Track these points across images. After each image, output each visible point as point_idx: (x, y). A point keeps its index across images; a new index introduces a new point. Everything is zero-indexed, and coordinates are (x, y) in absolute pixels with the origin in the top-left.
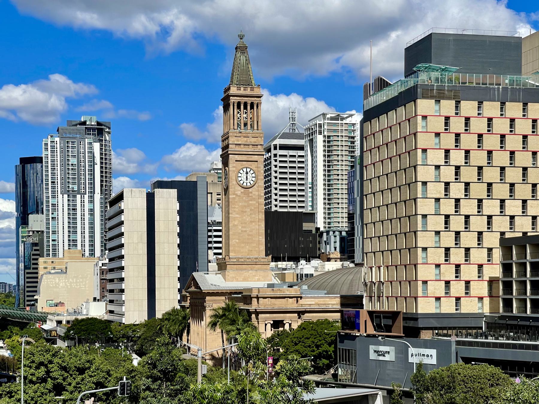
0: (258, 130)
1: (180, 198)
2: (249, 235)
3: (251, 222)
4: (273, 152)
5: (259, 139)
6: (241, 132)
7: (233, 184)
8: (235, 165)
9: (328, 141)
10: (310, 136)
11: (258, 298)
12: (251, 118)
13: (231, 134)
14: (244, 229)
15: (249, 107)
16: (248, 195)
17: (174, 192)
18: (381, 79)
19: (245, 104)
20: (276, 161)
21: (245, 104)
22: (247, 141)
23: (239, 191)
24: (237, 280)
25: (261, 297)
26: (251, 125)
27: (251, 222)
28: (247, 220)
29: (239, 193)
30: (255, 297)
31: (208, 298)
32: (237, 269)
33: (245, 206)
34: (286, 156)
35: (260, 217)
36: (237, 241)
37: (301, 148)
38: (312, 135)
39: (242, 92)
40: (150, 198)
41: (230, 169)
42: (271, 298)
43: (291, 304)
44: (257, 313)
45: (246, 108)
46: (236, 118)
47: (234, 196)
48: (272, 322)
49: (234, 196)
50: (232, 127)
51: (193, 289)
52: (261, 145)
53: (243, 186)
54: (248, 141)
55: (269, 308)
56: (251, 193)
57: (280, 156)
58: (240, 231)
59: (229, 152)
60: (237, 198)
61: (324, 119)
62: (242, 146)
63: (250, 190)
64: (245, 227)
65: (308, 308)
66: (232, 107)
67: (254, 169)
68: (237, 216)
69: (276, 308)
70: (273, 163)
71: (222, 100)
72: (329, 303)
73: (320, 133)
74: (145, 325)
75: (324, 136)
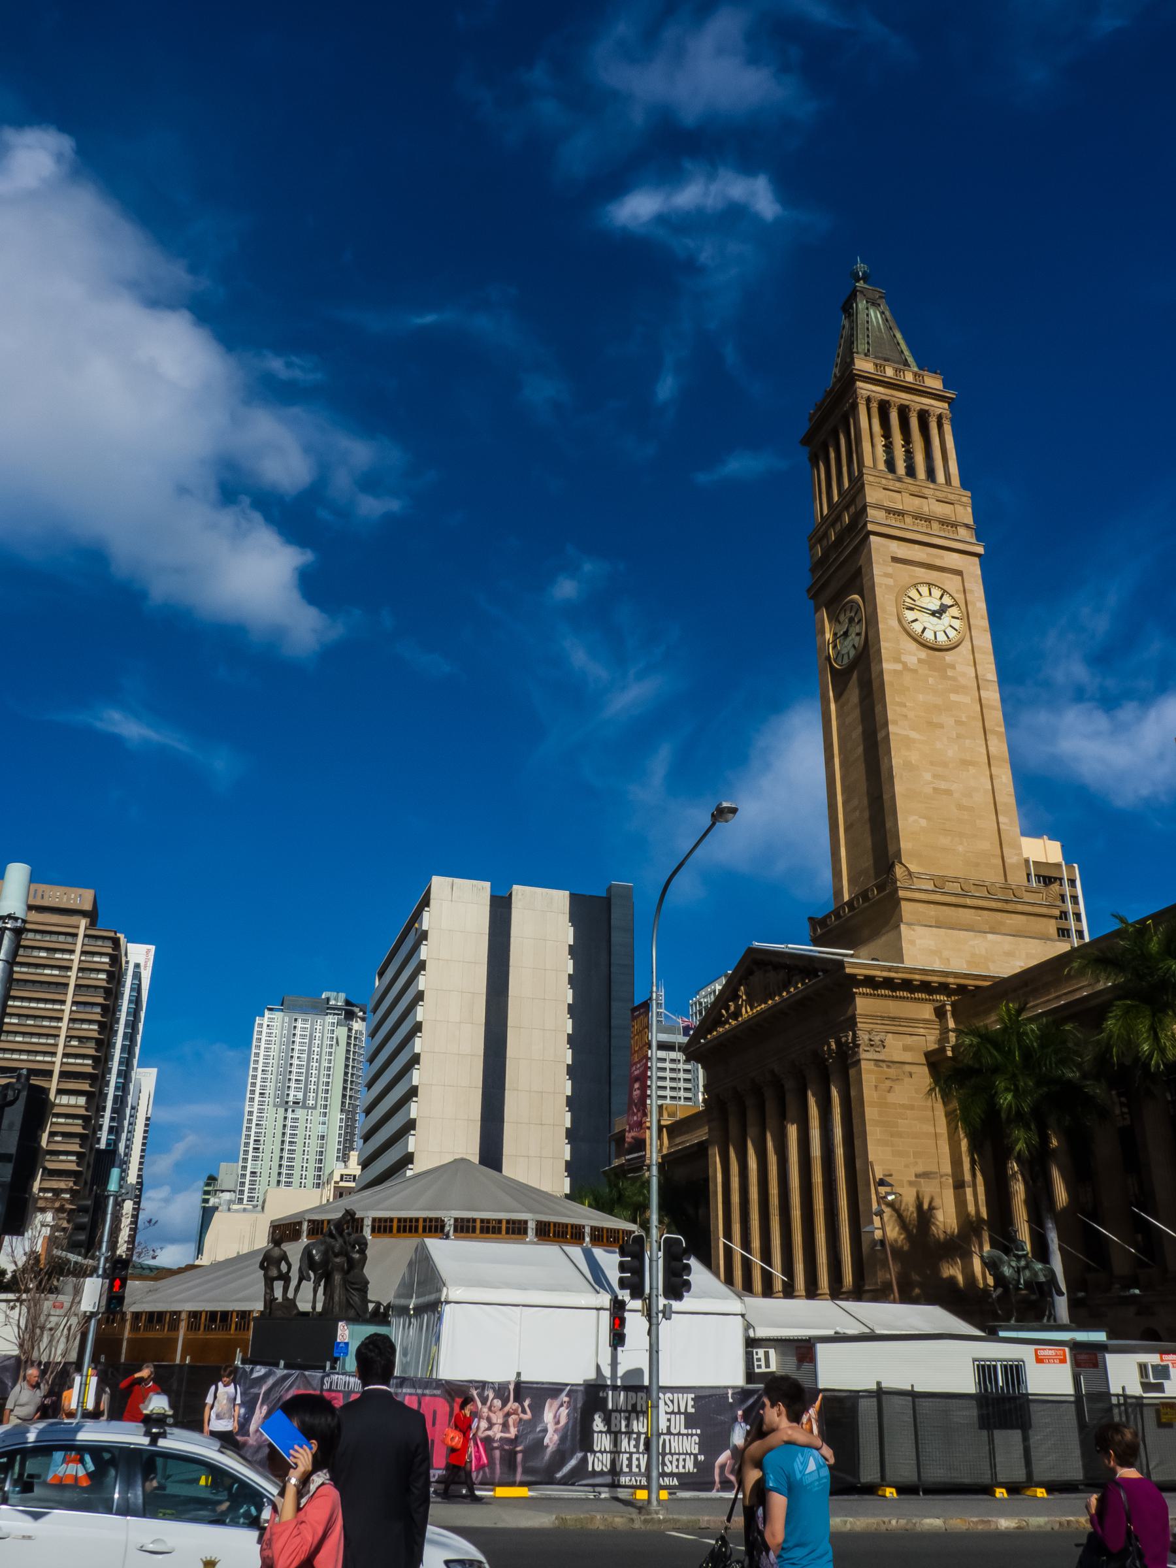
1: (576, 917)
2: (960, 807)
3: (965, 763)
5: (959, 508)
8: (890, 570)
13: (871, 479)
14: (943, 785)
16: (943, 670)
17: (561, 898)
19: (904, 411)
21: (904, 411)
23: (913, 655)
27: (965, 763)
28: (950, 753)
36: (923, 823)
40: (501, 910)
47: (899, 667)
49: (899, 667)
52: (967, 526)
58: (928, 790)
60: (907, 679)
62: (908, 520)
63: (949, 657)
68: (913, 735)
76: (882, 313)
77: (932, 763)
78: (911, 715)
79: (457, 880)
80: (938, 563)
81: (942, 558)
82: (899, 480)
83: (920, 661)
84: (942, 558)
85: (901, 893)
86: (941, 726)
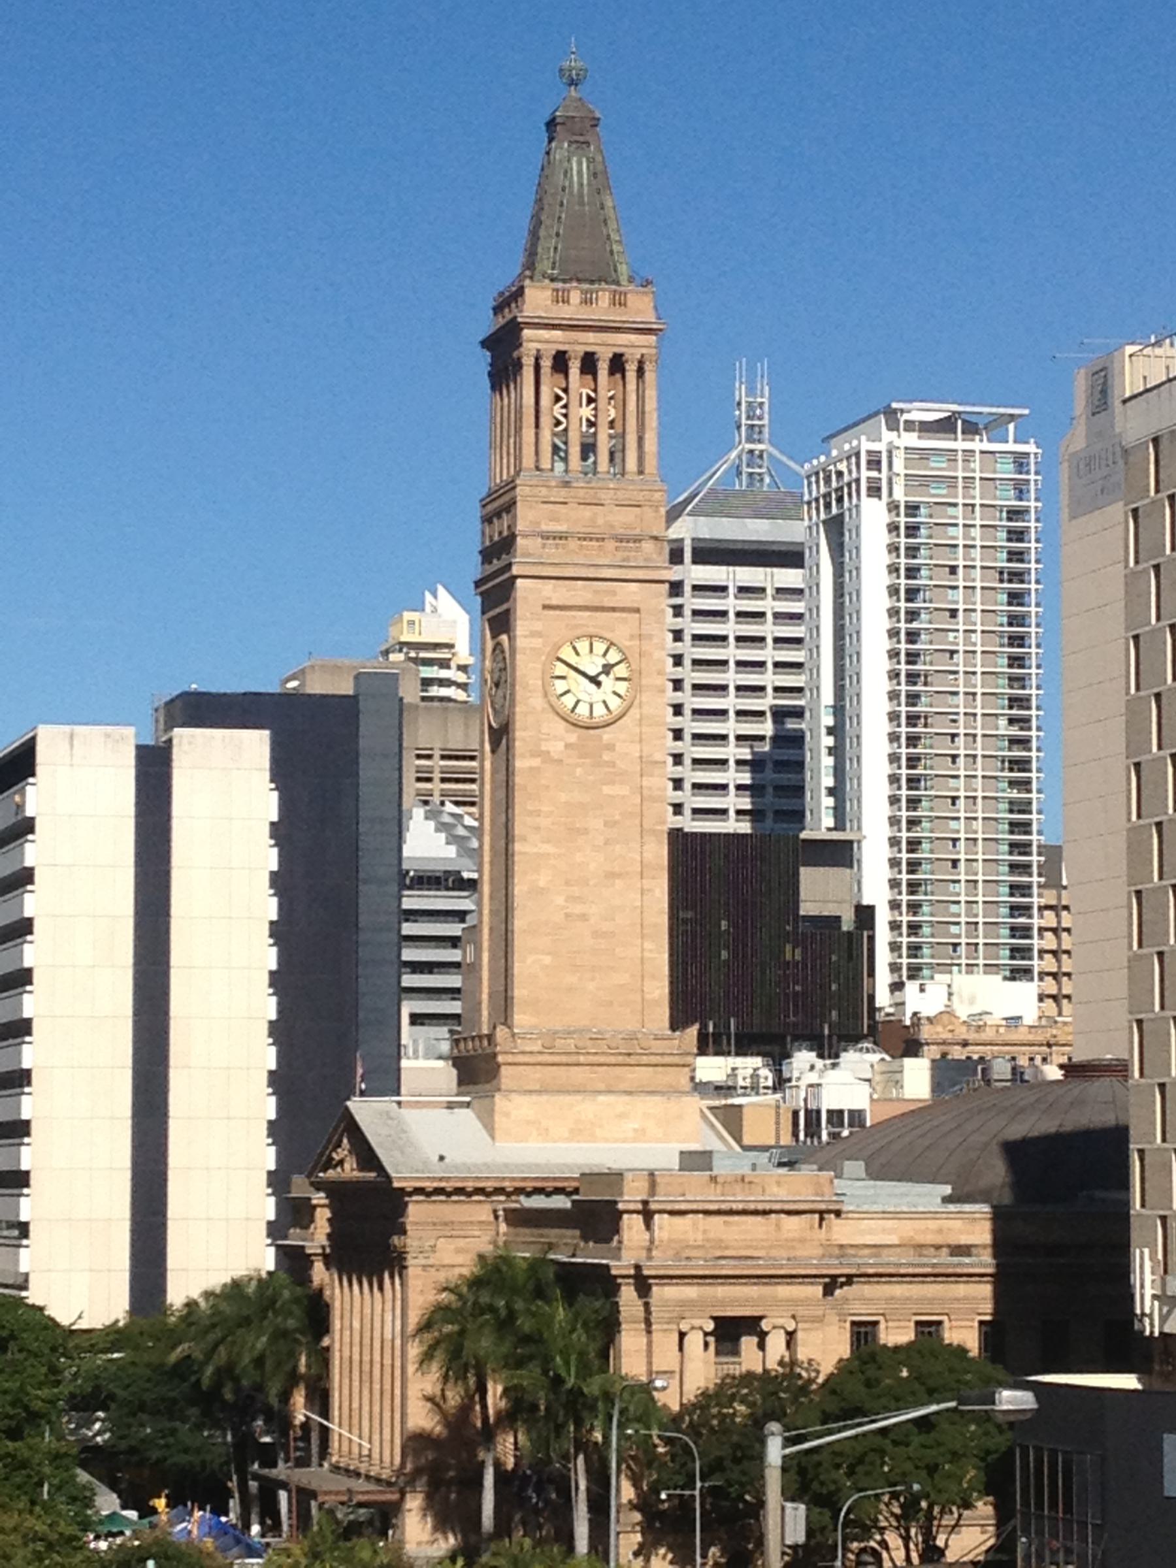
3: (612, 875)
5: (648, 512)
8: (538, 626)
12: (612, 424)
14: (578, 909)
26: (612, 454)
27: (612, 875)
29: (556, 748)
39: (573, 310)
46: (546, 422)
49: (536, 762)
50: (528, 460)
51: (349, 1170)
53: (573, 718)
54: (600, 521)
56: (610, 747)
59: (515, 570)
63: (607, 735)
71: (484, 344)
77: (567, 883)
78: (544, 822)
80: (607, 602)
81: (614, 593)
82: (566, 484)
83: (568, 746)
84: (614, 593)
85: (500, 1059)
86: (586, 831)
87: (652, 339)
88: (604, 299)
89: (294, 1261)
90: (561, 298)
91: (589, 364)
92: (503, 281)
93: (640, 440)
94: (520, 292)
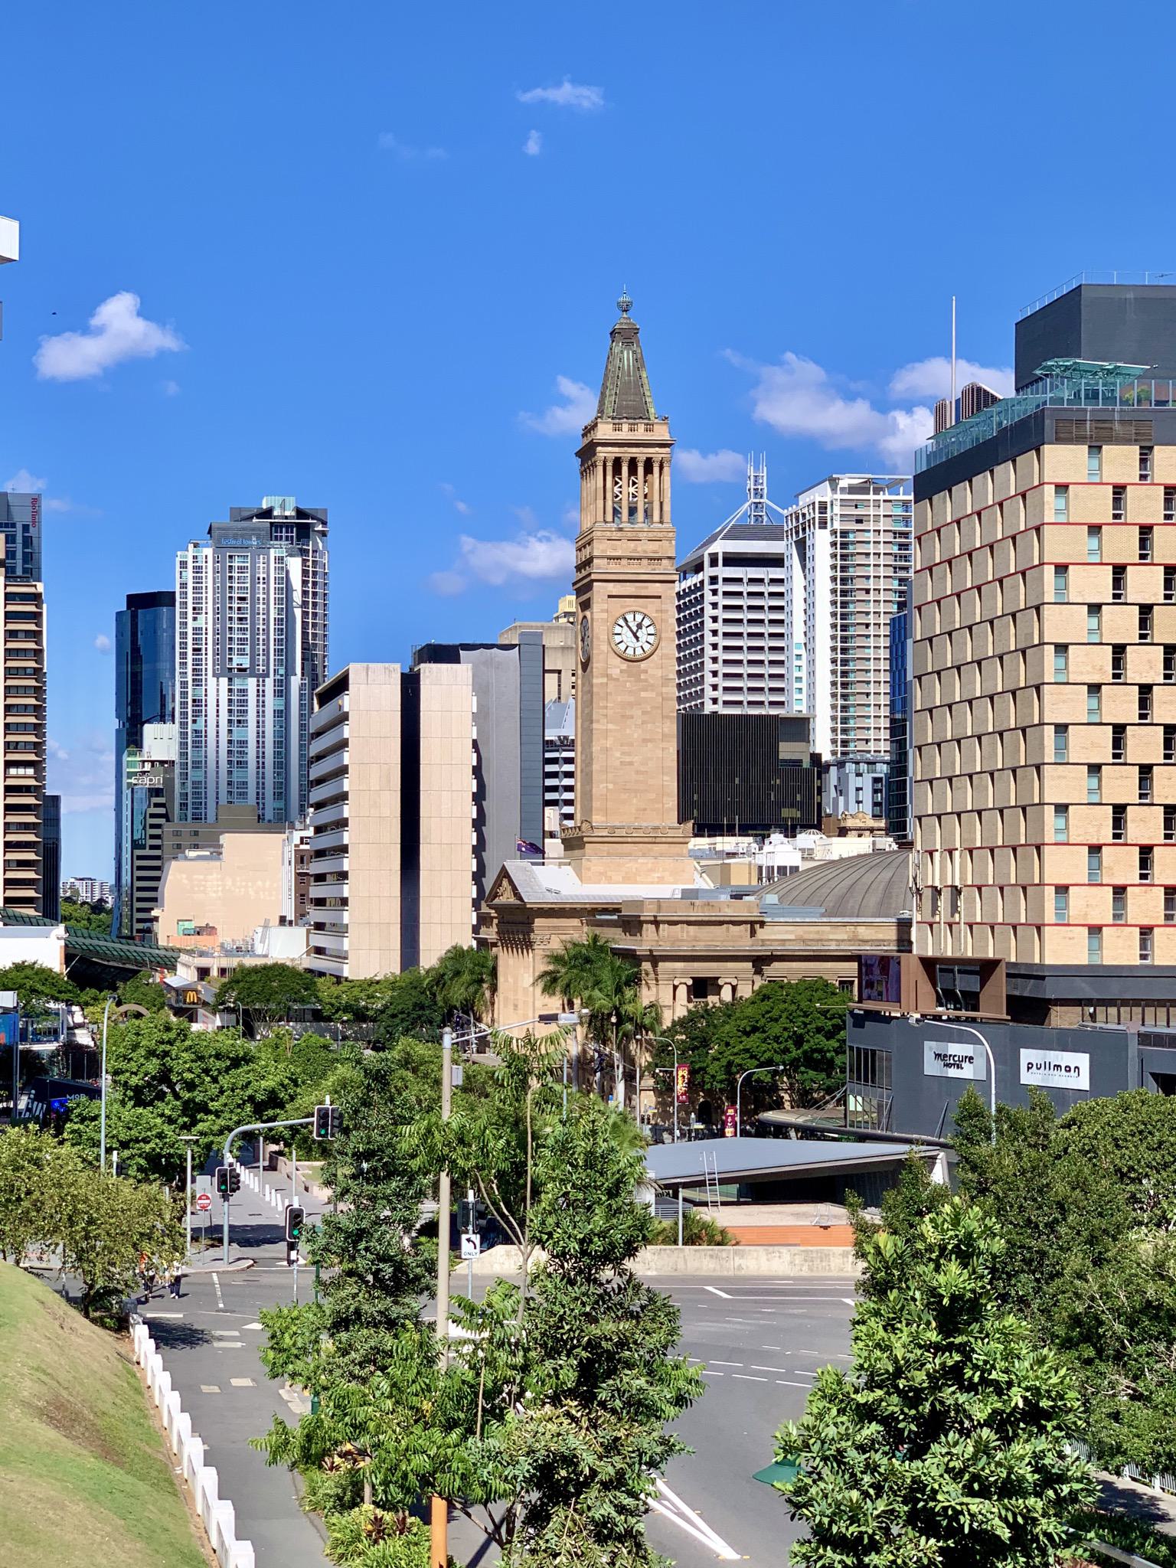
0: (661, 522)
2: (638, 772)
3: (645, 741)
4: (709, 571)
5: (665, 543)
6: (621, 530)
7: (600, 650)
9: (843, 543)
10: (797, 533)
11: (656, 923)
12: (646, 496)
14: (628, 759)
15: (641, 470)
18: (979, 389)
19: (633, 463)
20: (715, 592)
21: (633, 463)
22: (635, 550)
23: (617, 666)
24: (610, 880)
25: (664, 922)
26: (646, 511)
27: (645, 741)
29: (615, 672)
30: (651, 922)
31: (538, 922)
32: (609, 855)
33: (631, 705)
34: (740, 580)
35: (666, 730)
36: (611, 786)
37: (777, 561)
38: (804, 529)
40: (410, 687)
41: (595, 616)
42: (689, 923)
43: (738, 940)
44: (655, 959)
45: (633, 471)
47: (605, 680)
48: (690, 982)
49: (605, 680)
55: (685, 948)
57: (725, 580)
60: (611, 685)
61: (834, 490)
63: (643, 665)
64: (629, 754)
65: (778, 948)
66: (600, 469)
67: (653, 615)
69: (700, 948)
70: (709, 598)
72: (831, 937)
73: (823, 524)
74: (392, 984)
75: (834, 532)
76: (634, 352)
78: (610, 712)
79: (371, 665)
86: (632, 717)
87: (667, 450)
88: (641, 427)
89: (482, 943)
90: (617, 428)
91: (633, 463)
92: (587, 421)
93: (661, 504)
94: (596, 425)
